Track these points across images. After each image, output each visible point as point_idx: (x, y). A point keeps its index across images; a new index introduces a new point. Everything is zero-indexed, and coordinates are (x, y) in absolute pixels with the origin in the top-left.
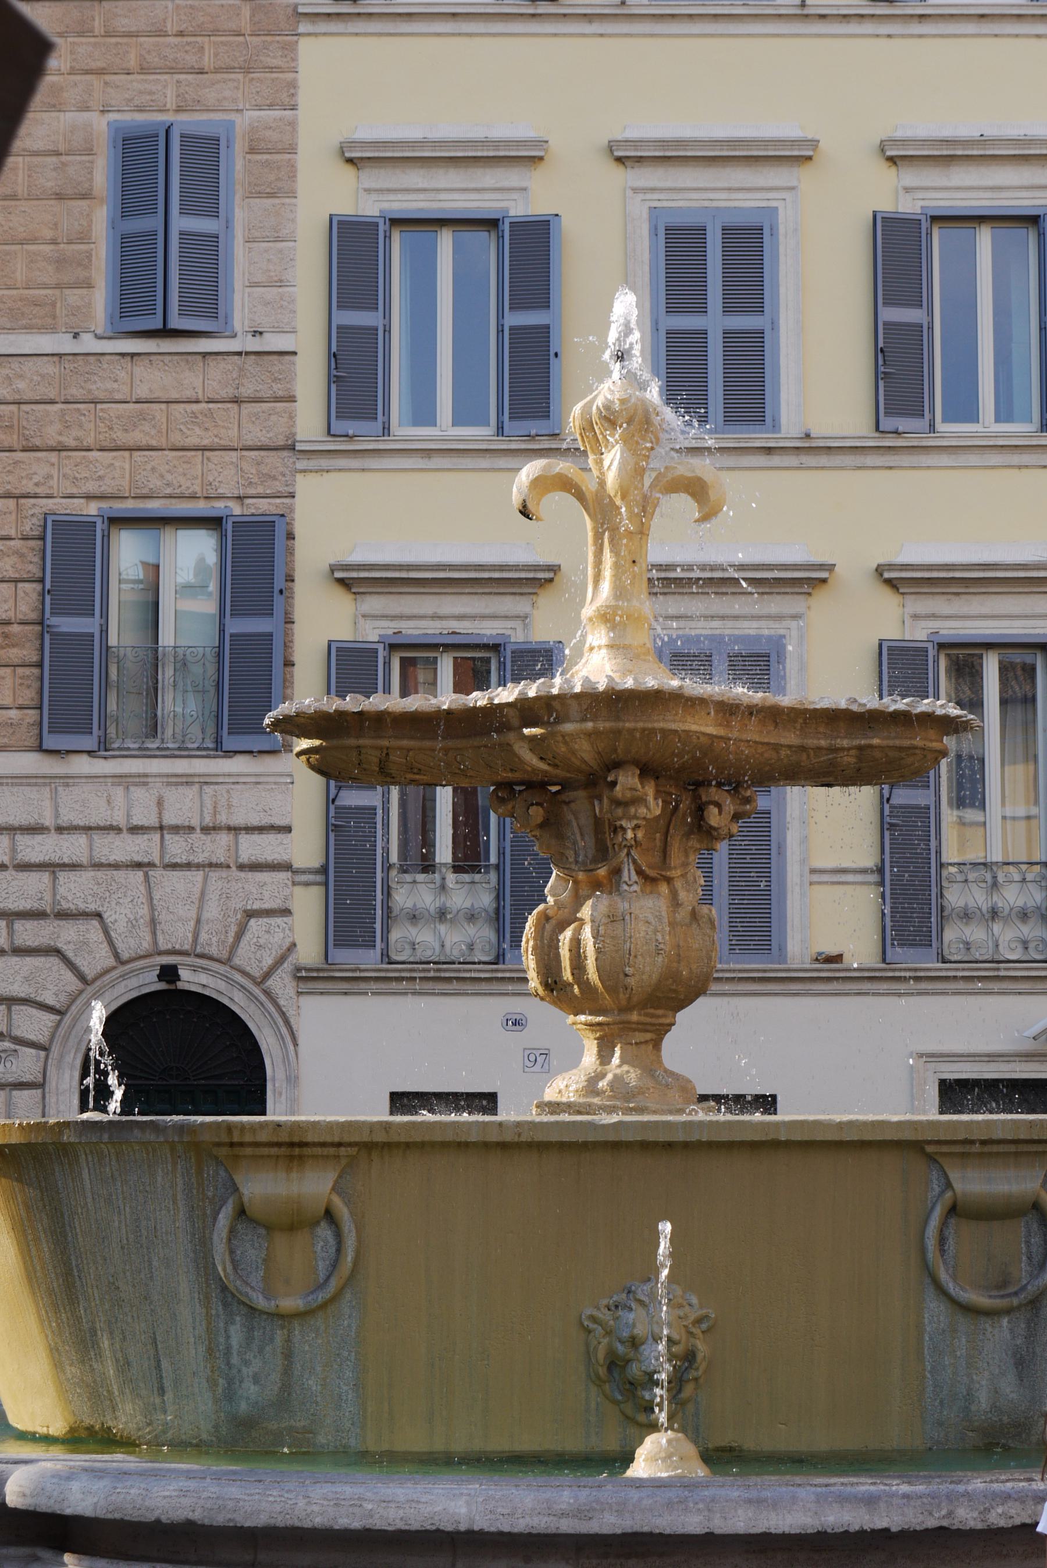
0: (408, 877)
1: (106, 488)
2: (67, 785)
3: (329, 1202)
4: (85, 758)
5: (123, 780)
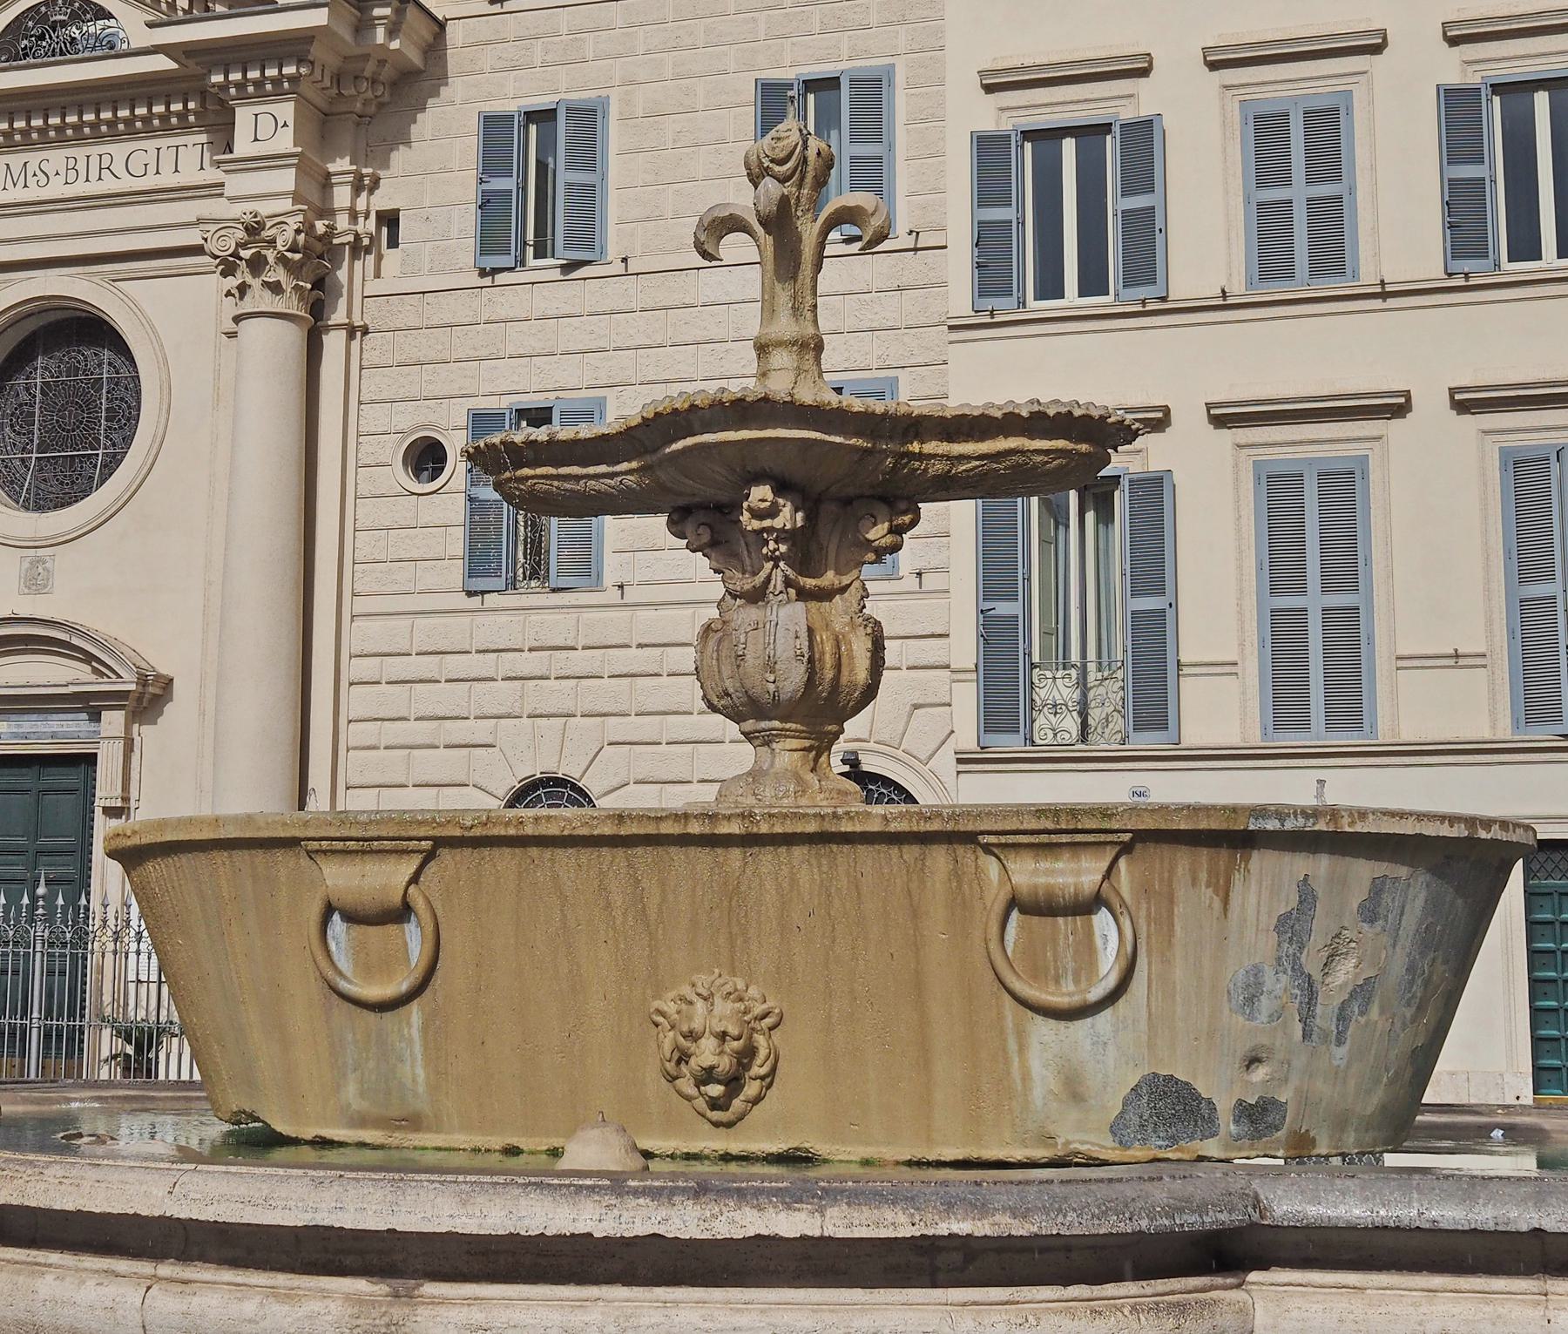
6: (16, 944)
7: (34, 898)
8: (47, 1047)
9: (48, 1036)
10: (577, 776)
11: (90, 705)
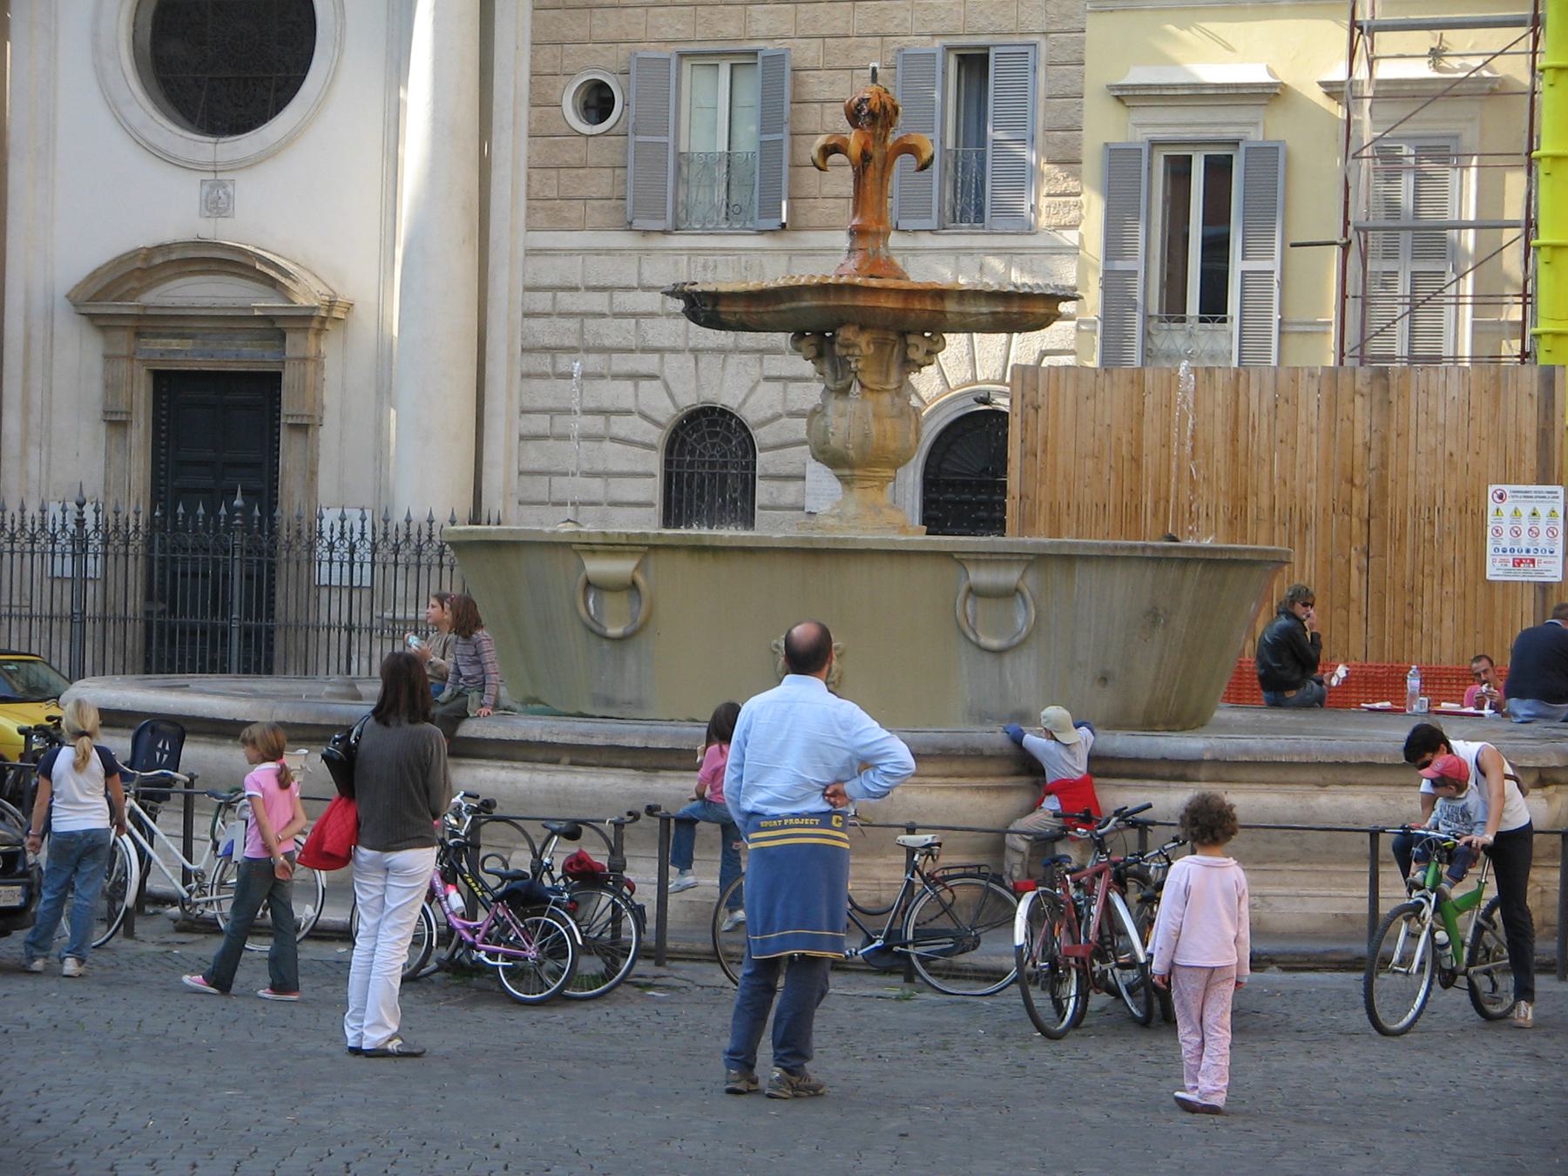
0: (1165, 326)
1: (945, 29)
2: (915, 255)
3: (633, 576)
4: (928, 235)
5: (956, 251)
6: (195, 550)
7: (231, 510)
8: (247, 646)
9: (247, 635)
10: (735, 406)
11: (275, 328)
